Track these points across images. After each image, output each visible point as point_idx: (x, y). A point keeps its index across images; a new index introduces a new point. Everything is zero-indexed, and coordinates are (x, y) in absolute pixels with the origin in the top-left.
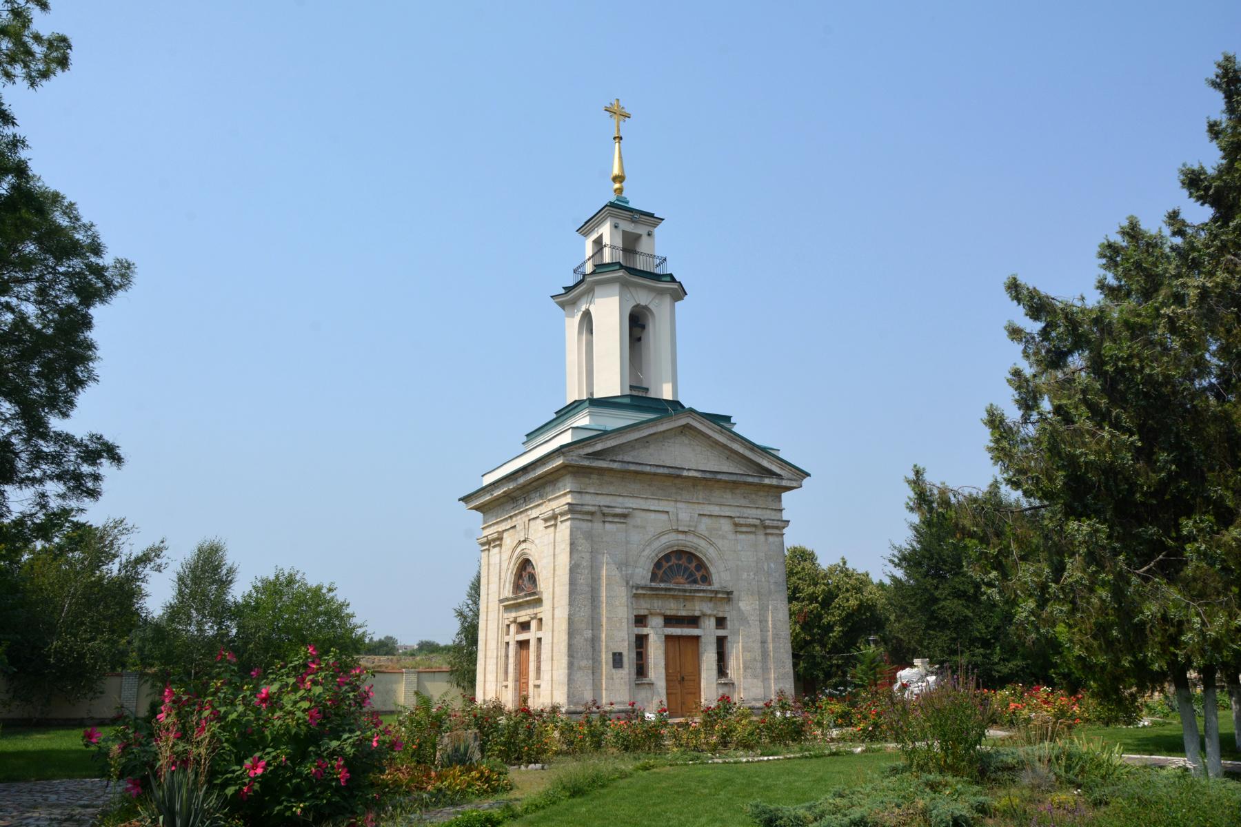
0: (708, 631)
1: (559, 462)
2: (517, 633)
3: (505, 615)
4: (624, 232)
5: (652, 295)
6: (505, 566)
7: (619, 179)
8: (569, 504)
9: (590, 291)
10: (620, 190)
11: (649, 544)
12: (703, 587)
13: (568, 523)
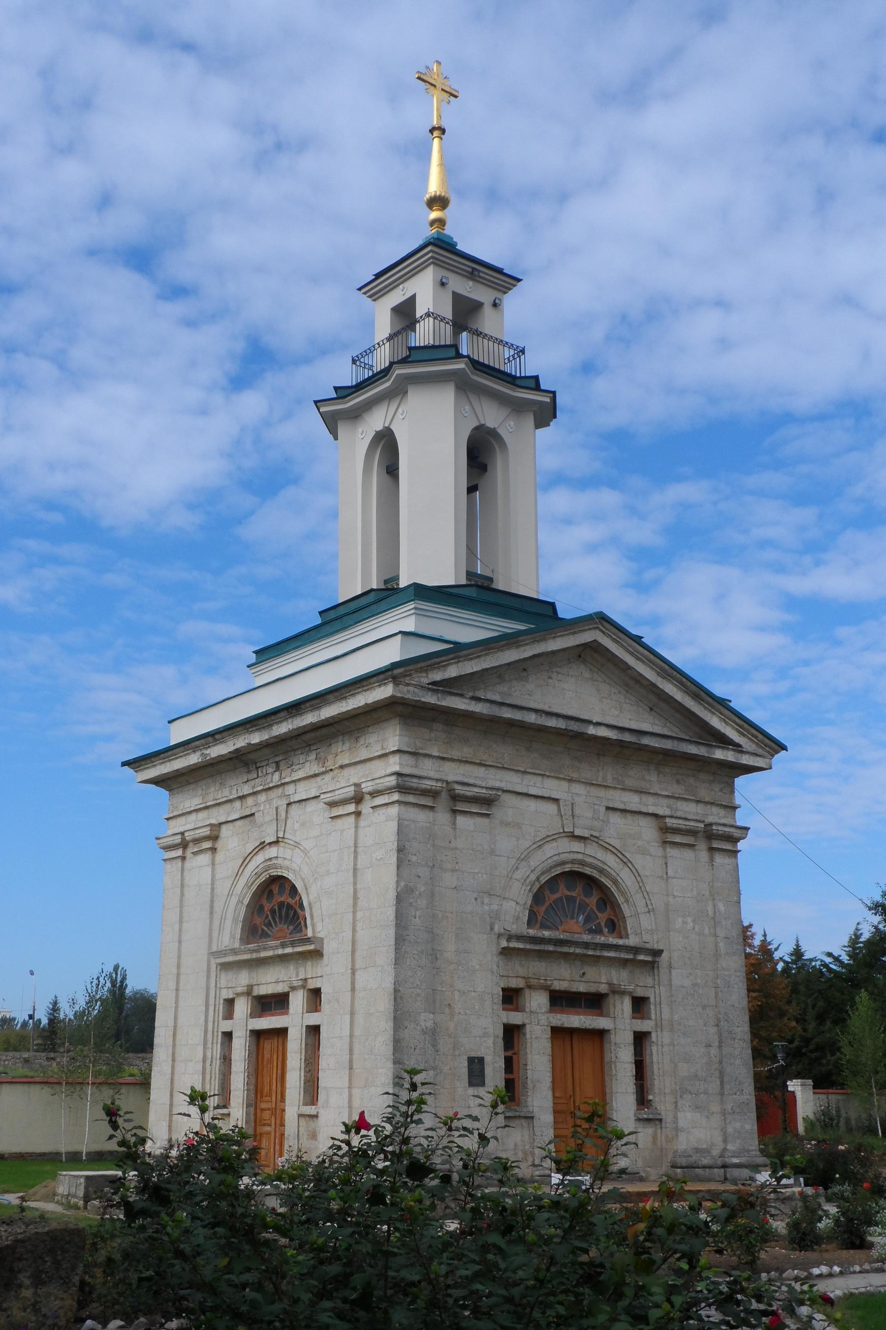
0: (620, 1022)
1: (383, 692)
2: (253, 1015)
3: (225, 979)
4: (456, 296)
5: (504, 412)
6: (223, 888)
7: (439, 202)
8: (398, 774)
9: (398, 392)
10: (441, 222)
11: (525, 858)
12: (612, 940)
13: (394, 810)
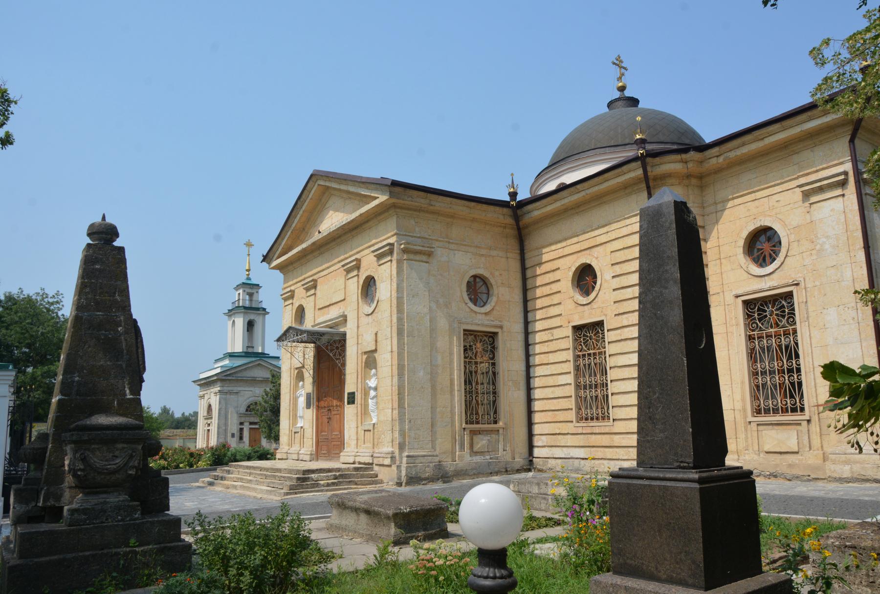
7: (248, 270)
